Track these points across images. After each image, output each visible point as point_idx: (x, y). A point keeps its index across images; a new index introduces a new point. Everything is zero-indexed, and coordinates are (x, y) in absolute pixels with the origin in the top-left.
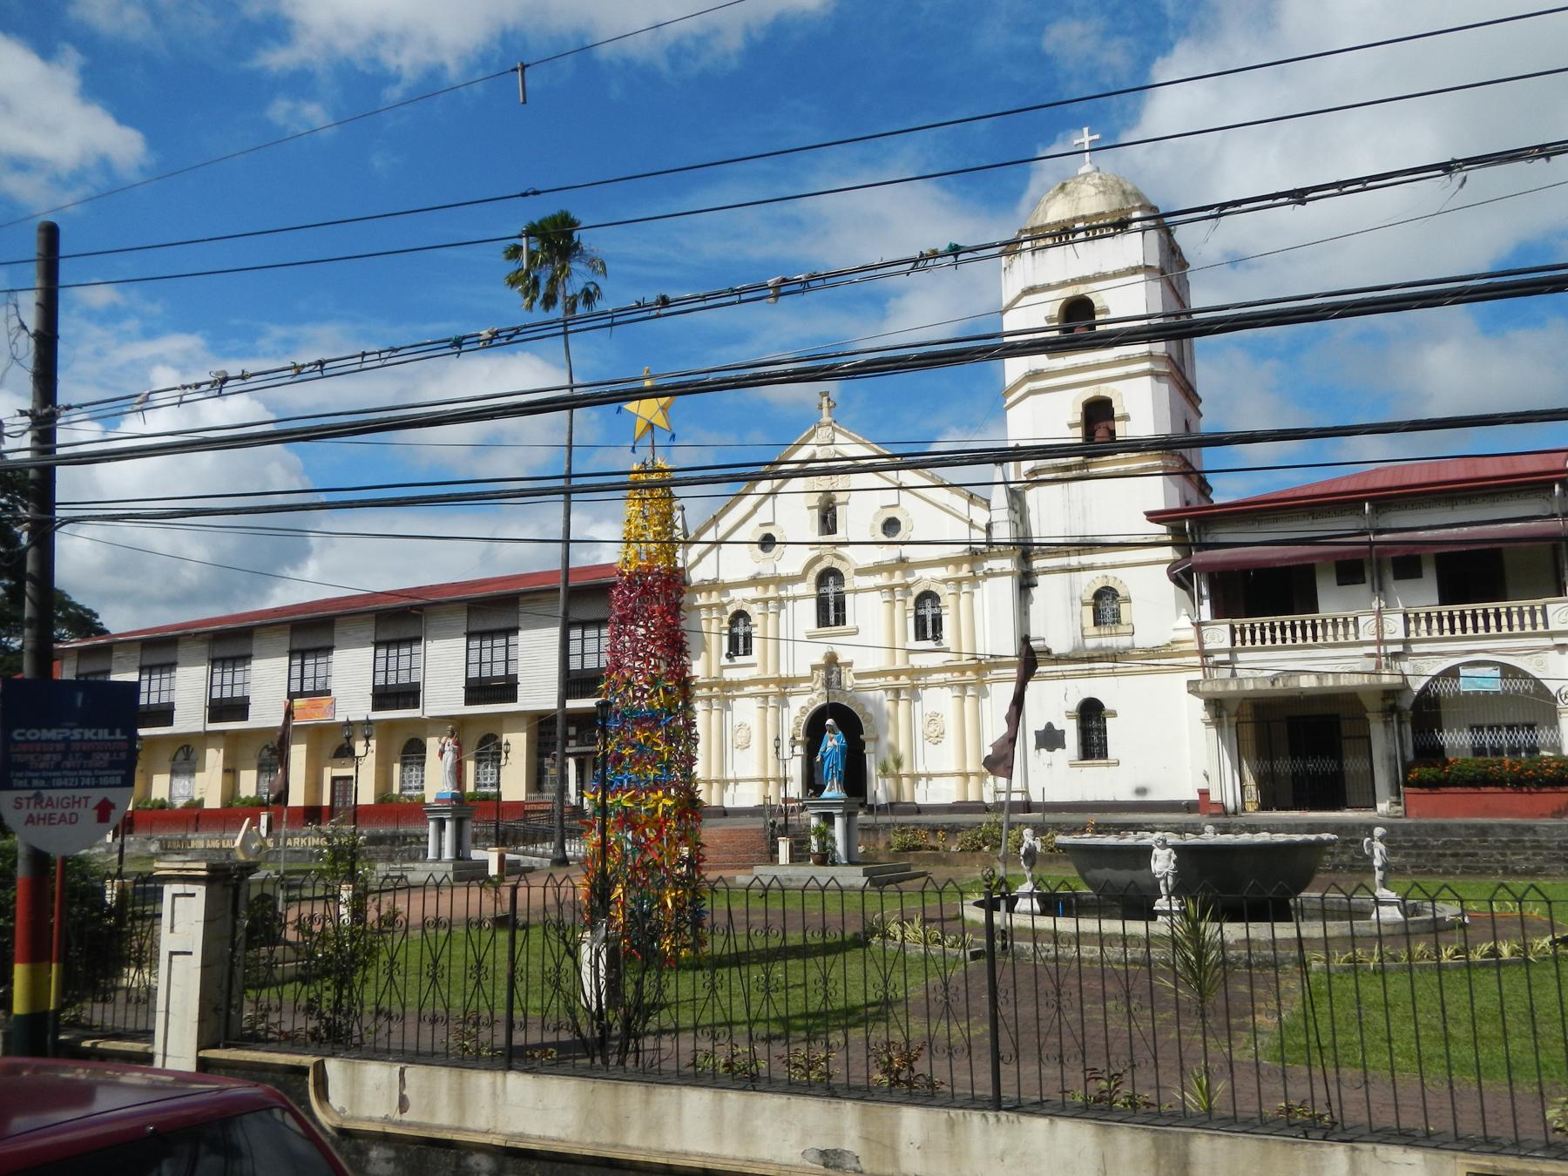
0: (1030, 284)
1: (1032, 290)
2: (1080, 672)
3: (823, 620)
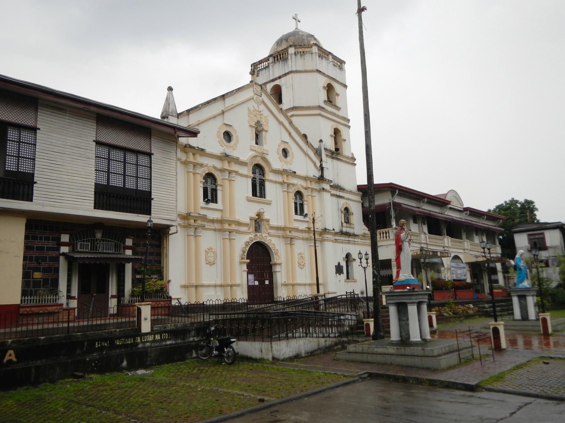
0: (319, 69)
1: (319, 71)
2: (347, 241)
3: (254, 194)
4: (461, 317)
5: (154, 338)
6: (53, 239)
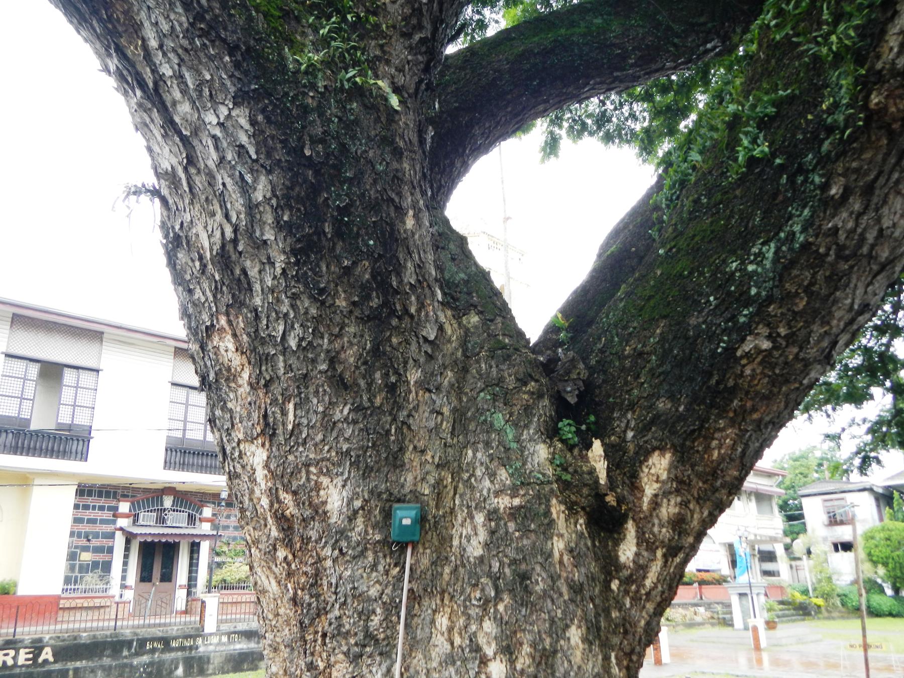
4: (678, 625)
5: (220, 640)
6: (110, 509)
